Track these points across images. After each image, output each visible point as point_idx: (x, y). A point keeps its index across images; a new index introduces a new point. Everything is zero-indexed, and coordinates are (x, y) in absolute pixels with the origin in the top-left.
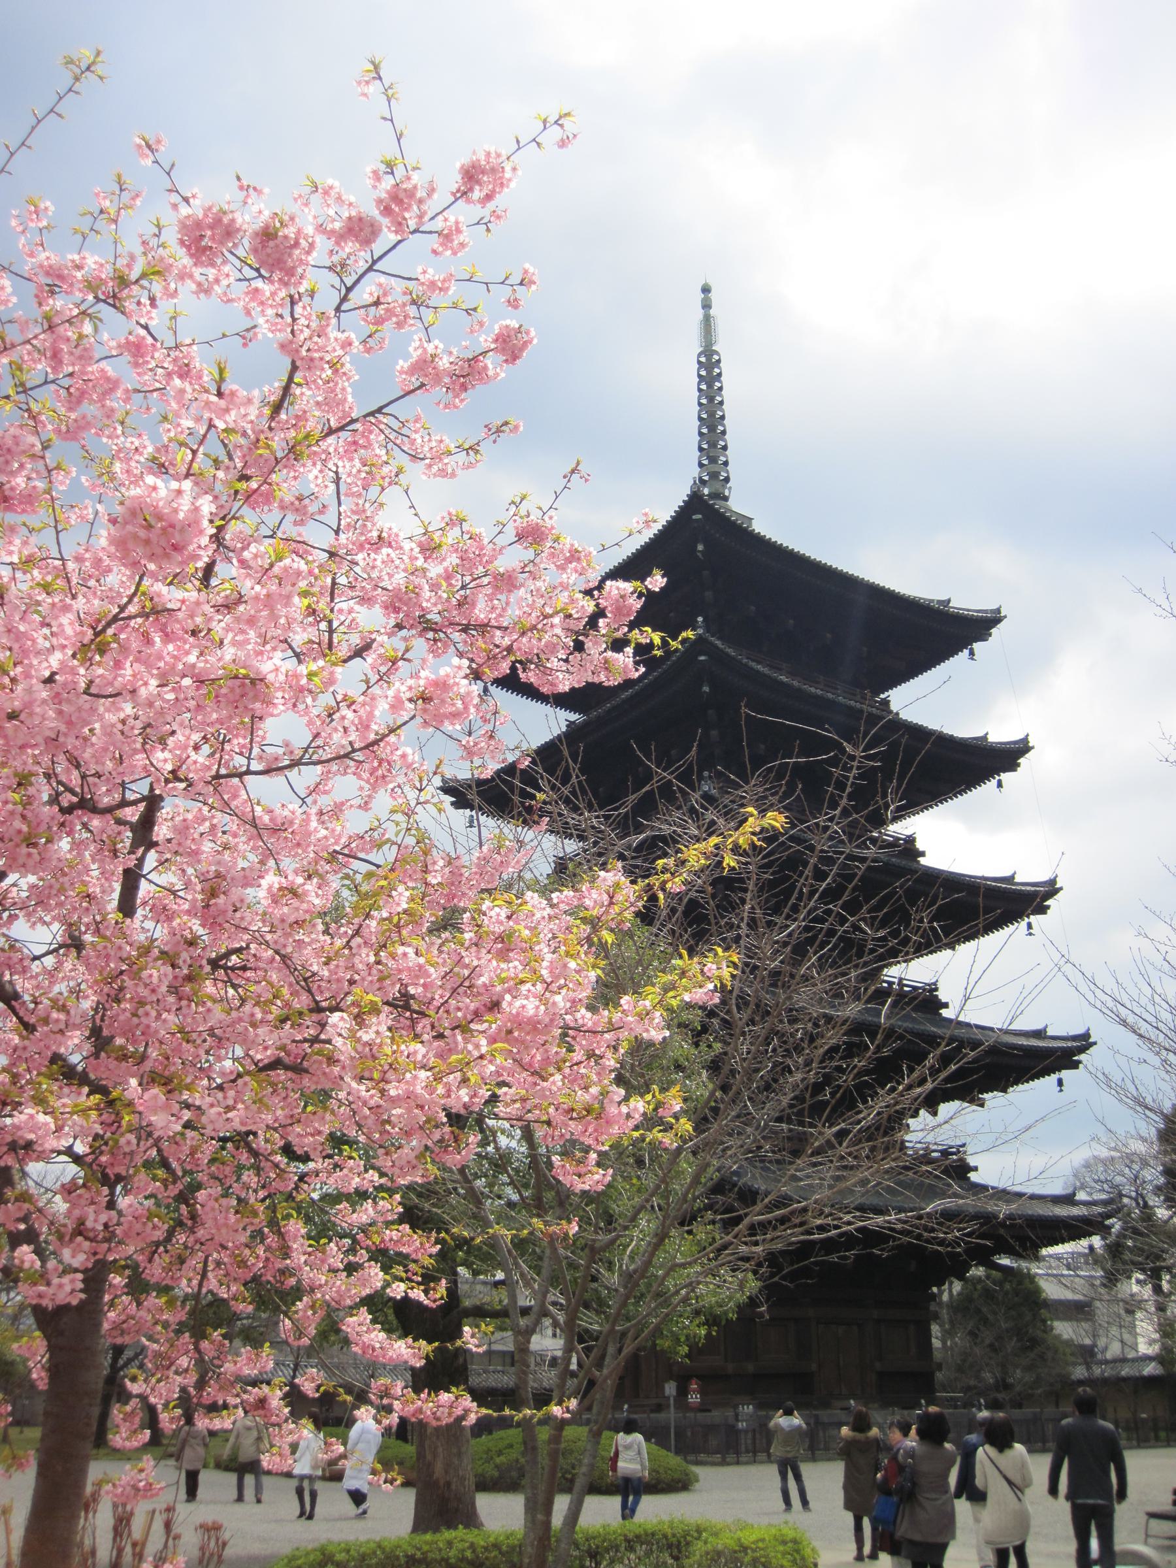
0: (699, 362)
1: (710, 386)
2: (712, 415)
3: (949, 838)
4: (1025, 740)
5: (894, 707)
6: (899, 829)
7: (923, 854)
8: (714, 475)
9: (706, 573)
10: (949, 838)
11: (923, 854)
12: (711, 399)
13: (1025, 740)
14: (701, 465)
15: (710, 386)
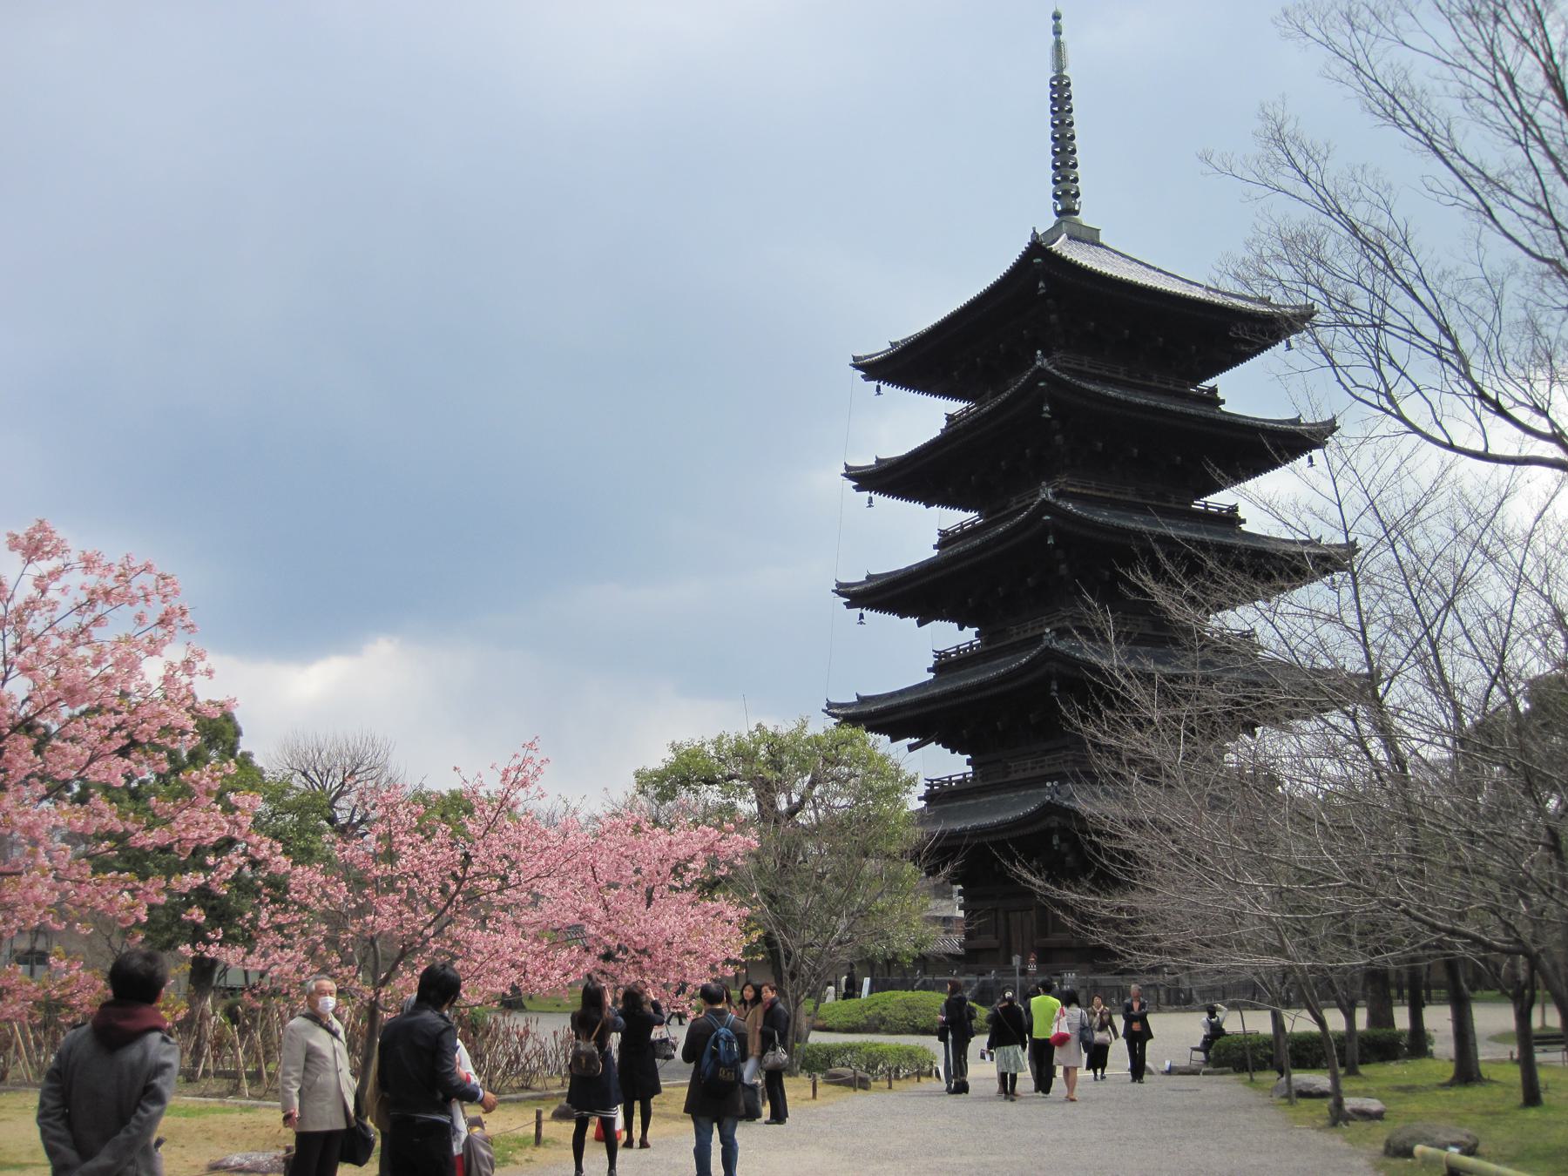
0: (1052, 86)
1: (1061, 109)
2: (1063, 136)
3: (1266, 504)
4: (1333, 420)
5: (1220, 395)
6: (1220, 499)
7: (1244, 521)
8: (1066, 192)
9: (1049, 301)
10: (1266, 504)
11: (1244, 521)
12: (1062, 122)
13: (1333, 420)
14: (1055, 182)
15: (1061, 109)
